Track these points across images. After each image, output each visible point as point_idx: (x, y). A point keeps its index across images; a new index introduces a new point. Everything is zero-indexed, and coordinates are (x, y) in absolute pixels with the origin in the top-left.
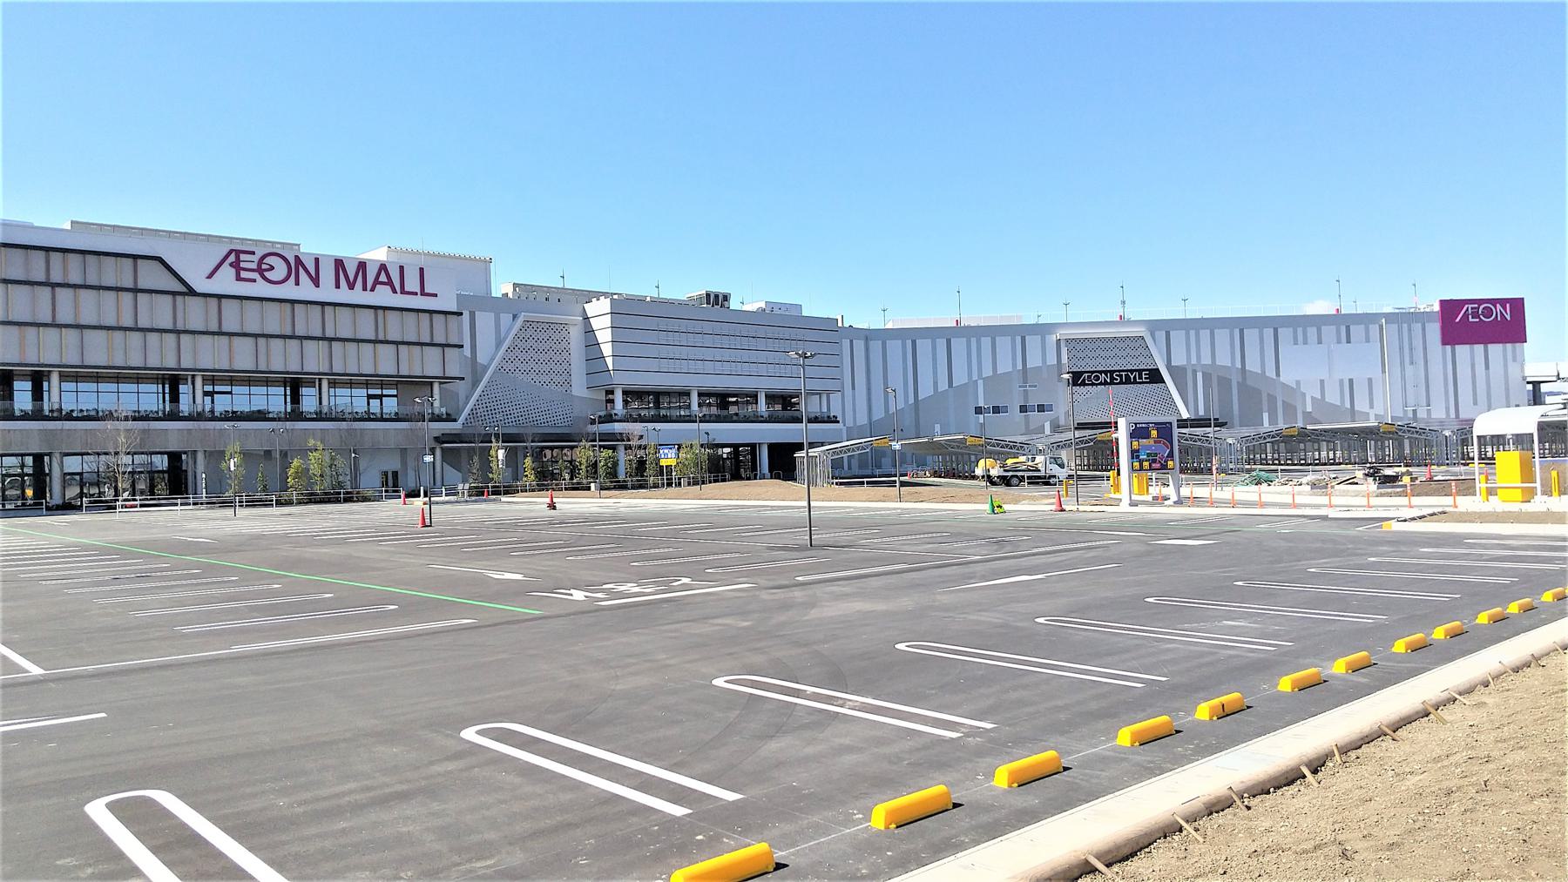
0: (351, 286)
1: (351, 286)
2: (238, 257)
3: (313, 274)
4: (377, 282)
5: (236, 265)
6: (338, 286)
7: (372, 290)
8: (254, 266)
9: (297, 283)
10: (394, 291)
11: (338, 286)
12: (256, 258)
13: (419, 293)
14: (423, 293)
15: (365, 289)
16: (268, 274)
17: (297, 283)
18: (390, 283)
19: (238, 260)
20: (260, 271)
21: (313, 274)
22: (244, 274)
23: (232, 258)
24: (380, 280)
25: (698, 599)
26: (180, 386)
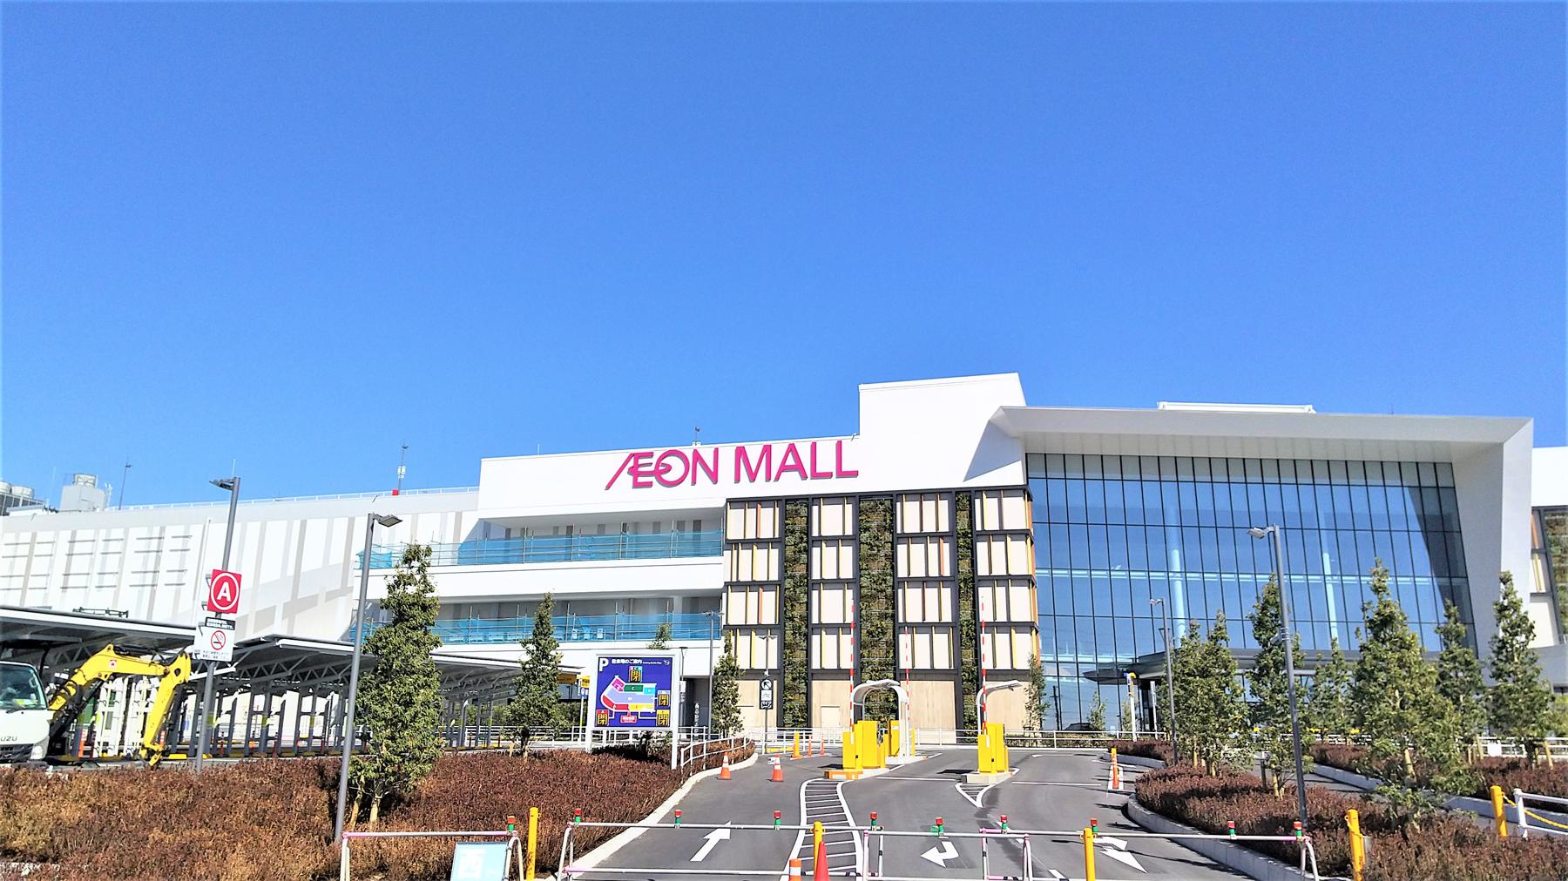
0: (753, 477)
1: (753, 477)
2: (636, 461)
3: (711, 466)
4: (784, 468)
5: (634, 472)
6: (737, 479)
7: (777, 478)
8: (652, 468)
9: (694, 482)
10: (804, 476)
11: (737, 479)
12: (654, 460)
13: (834, 475)
14: (842, 474)
15: (768, 478)
16: (666, 477)
17: (694, 482)
18: (799, 467)
19: (637, 465)
20: (657, 473)
21: (711, 466)
22: (641, 479)
23: (631, 463)
24: (787, 463)
25: (15, 668)
26: (899, 546)
